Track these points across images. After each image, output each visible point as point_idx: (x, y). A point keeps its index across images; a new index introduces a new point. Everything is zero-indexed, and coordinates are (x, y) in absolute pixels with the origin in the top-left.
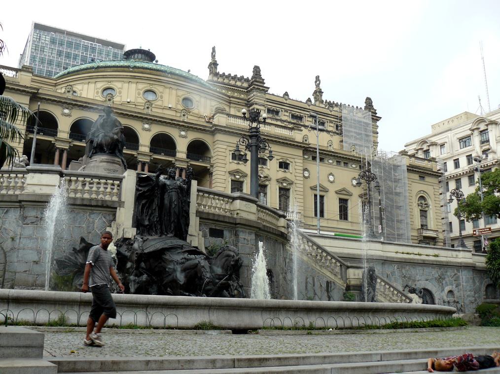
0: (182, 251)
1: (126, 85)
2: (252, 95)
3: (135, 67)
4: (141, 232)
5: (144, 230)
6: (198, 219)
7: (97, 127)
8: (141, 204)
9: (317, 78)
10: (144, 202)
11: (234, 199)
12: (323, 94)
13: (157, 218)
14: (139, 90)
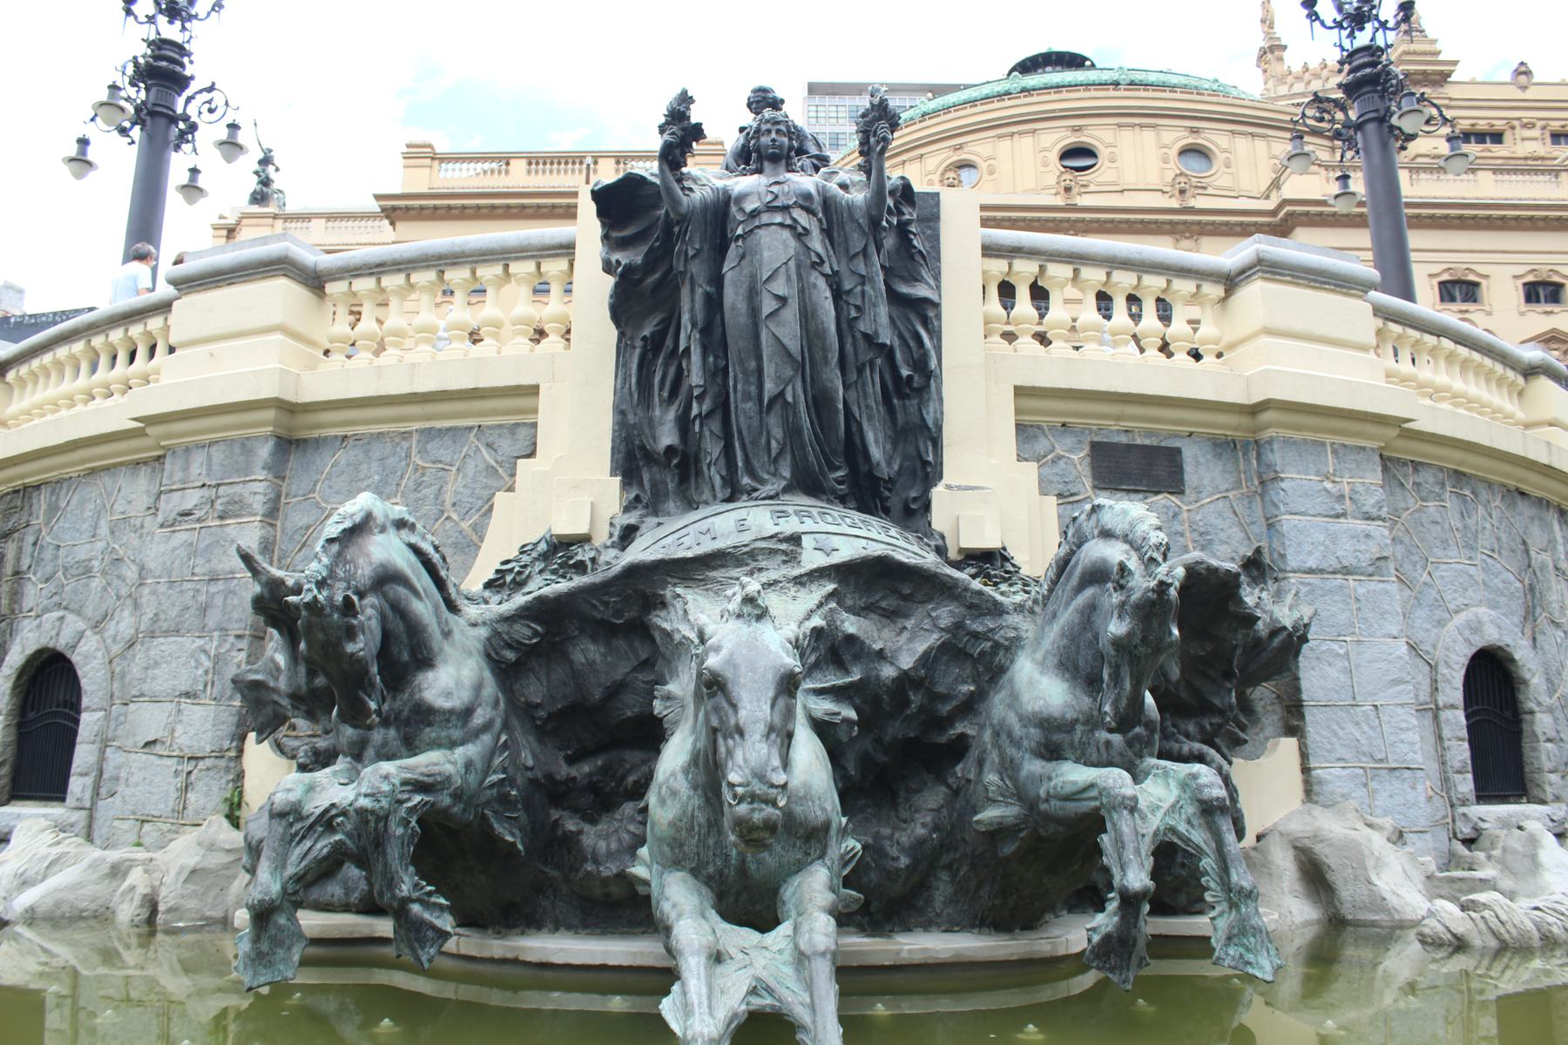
0: (796, 572)
1: (1005, 144)
4: (645, 498)
8: (639, 343)
10: (647, 332)
11: (1231, 281)
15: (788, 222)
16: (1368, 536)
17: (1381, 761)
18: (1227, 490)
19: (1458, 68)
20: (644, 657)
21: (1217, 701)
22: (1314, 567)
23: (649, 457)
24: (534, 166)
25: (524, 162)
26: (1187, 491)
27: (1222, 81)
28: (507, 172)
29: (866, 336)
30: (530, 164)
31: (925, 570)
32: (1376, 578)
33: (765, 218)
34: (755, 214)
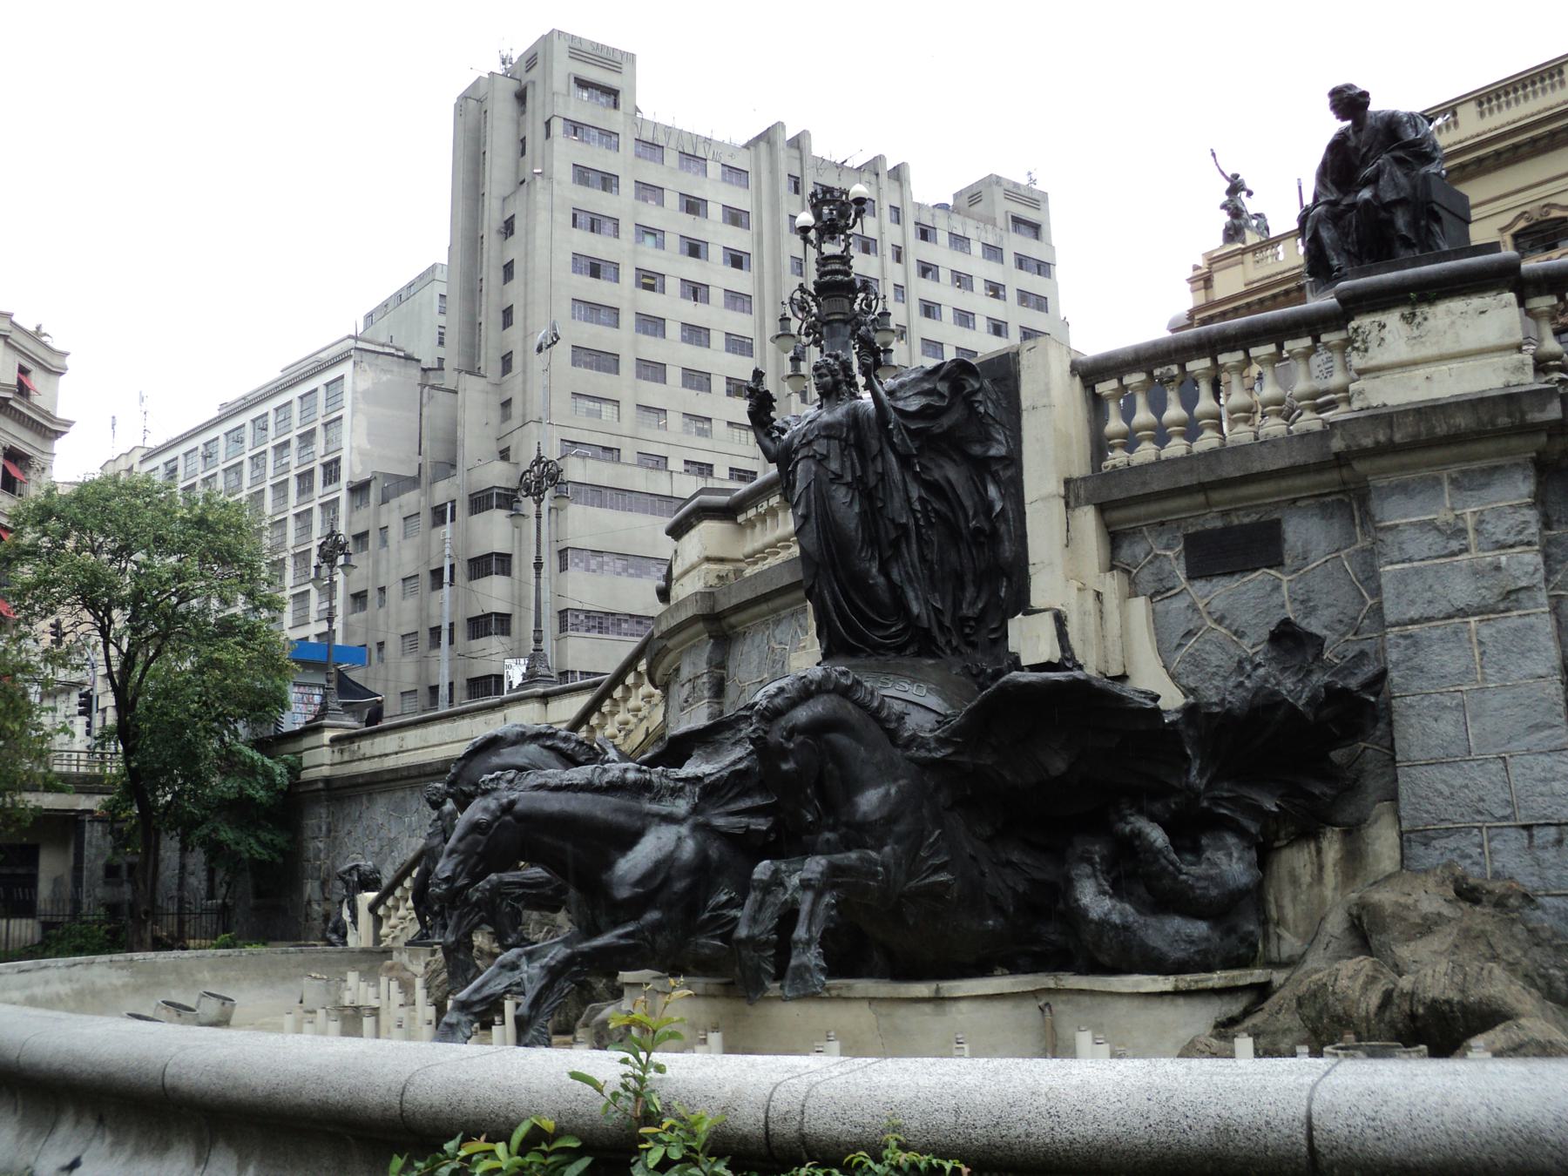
6: (1087, 518)
16: (1498, 568)
17: (1506, 818)
18: (1337, 550)
21: (1175, 783)
22: (1416, 617)
24: (1486, 106)
25: (1472, 107)
26: (1288, 561)
28: (1456, 123)
30: (1480, 104)
32: (1515, 613)
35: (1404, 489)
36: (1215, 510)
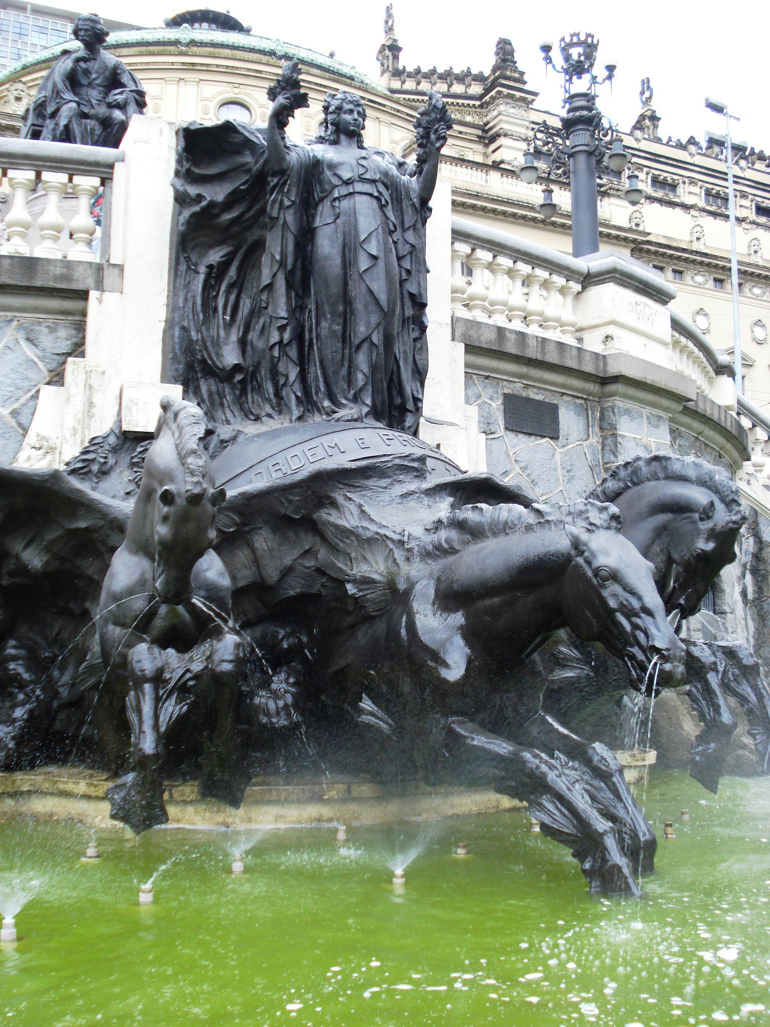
0: (425, 485)
1: (172, 88)
2: (495, 113)
3: (193, 43)
5: (222, 396)
7: (55, 85)
8: (202, 269)
9: (646, 85)
11: (589, 280)
12: (660, 123)
13: (282, 329)
14: (206, 99)
15: (376, 194)
19: (538, 99)
20: (307, 548)
23: (210, 370)
27: (357, 69)
29: (412, 296)
31: (511, 492)
33: (359, 187)
34: (347, 183)
35: (628, 412)
36: (524, 382)
